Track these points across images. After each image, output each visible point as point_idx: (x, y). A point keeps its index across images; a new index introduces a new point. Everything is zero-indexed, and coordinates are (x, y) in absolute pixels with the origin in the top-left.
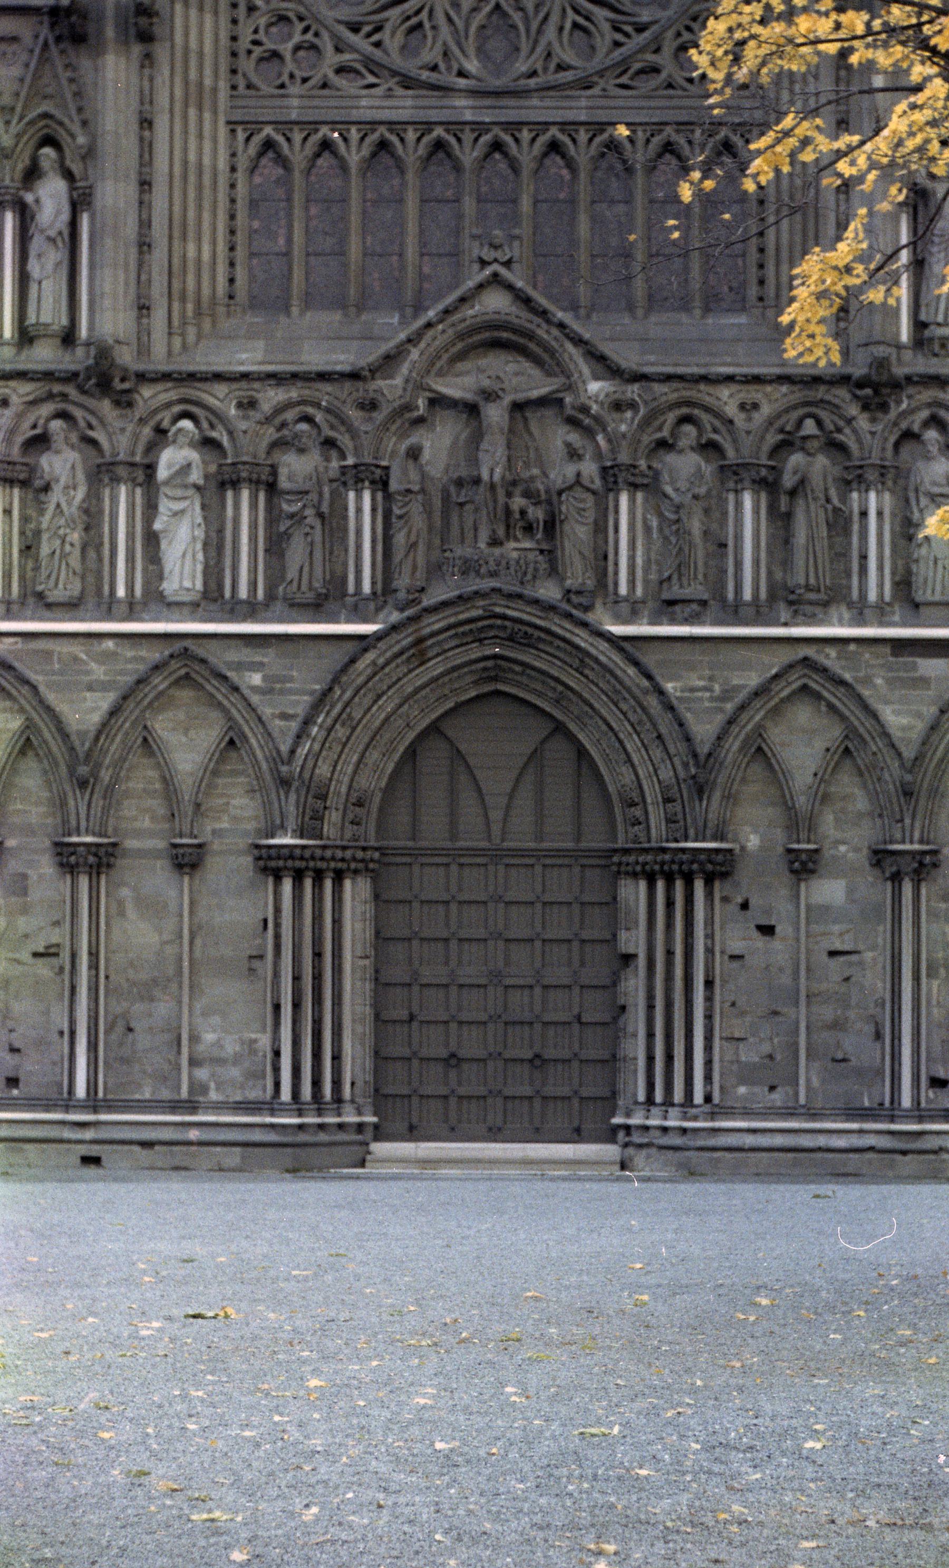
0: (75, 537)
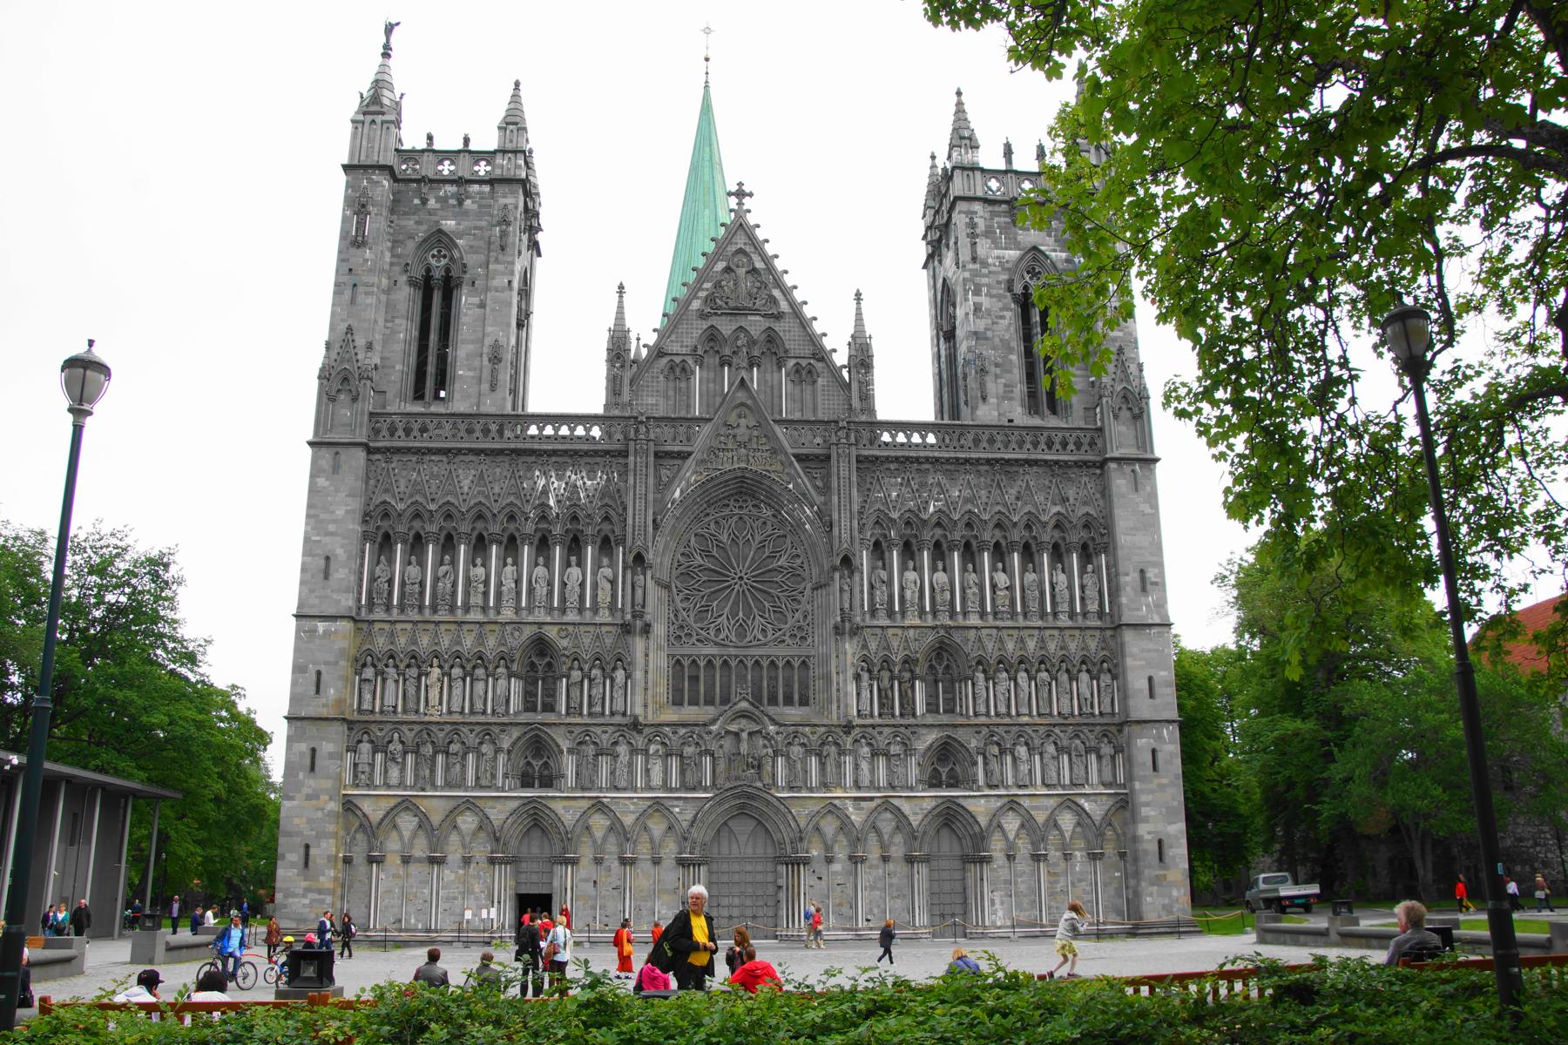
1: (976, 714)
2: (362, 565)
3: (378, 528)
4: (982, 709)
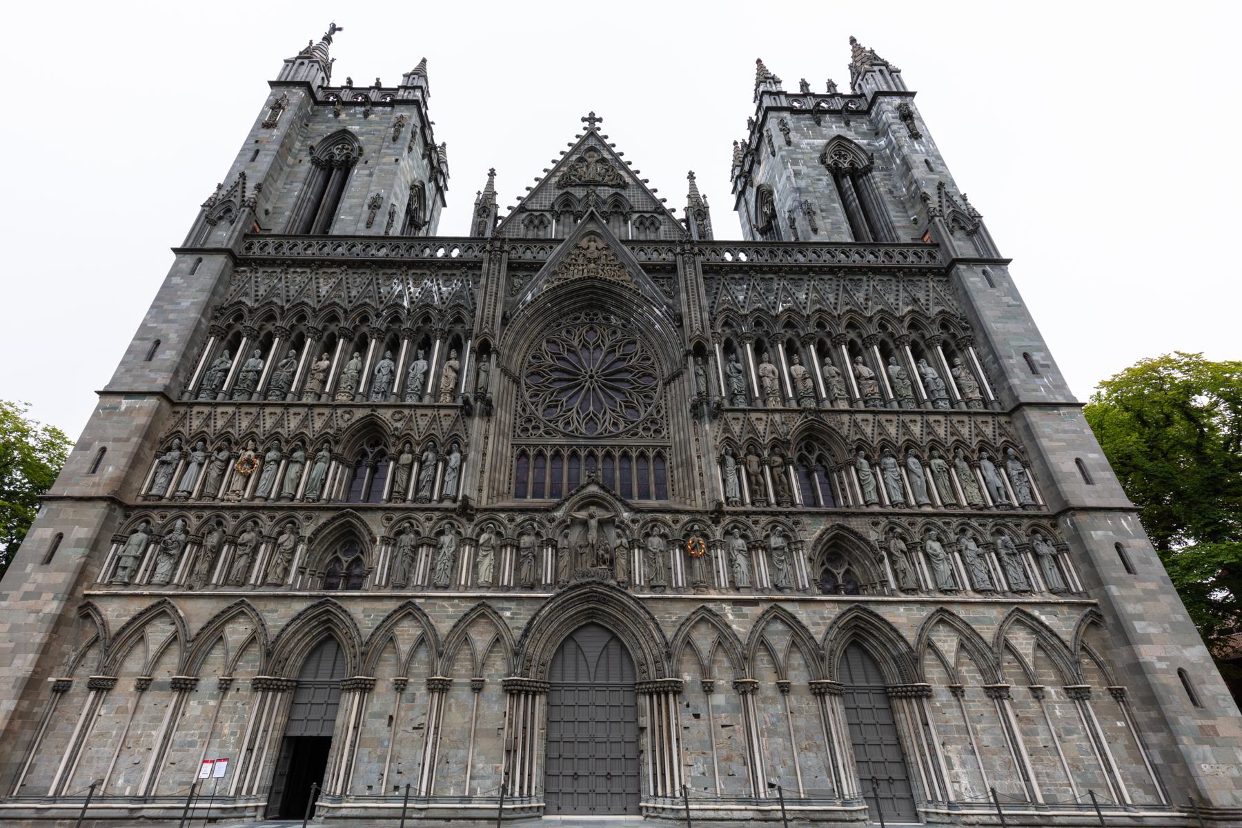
0: (449, 564)
1: (867, 504)
2: (200, 356)
3: (229, 326)
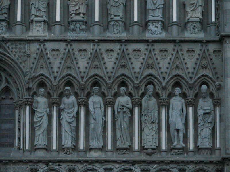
1: (34, 148)
4: (41, 141)
